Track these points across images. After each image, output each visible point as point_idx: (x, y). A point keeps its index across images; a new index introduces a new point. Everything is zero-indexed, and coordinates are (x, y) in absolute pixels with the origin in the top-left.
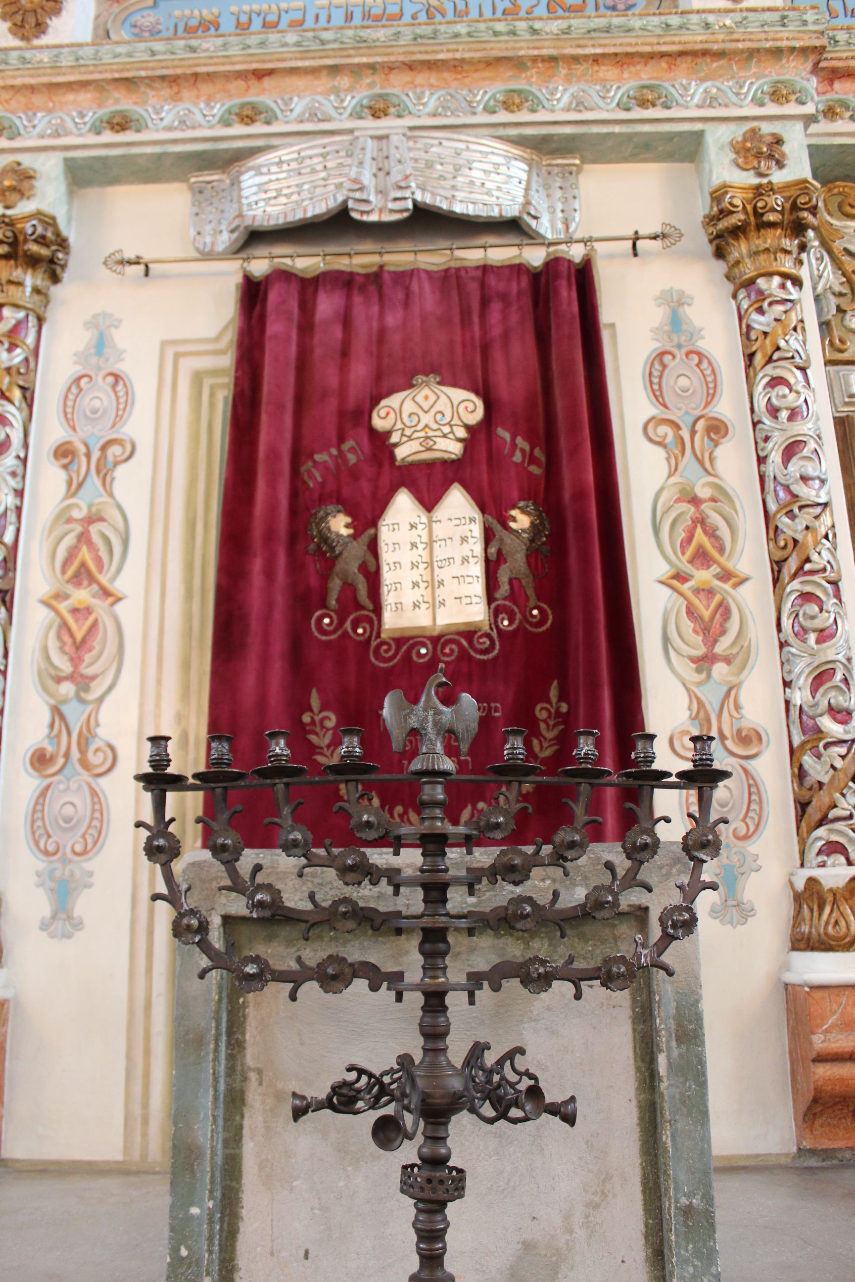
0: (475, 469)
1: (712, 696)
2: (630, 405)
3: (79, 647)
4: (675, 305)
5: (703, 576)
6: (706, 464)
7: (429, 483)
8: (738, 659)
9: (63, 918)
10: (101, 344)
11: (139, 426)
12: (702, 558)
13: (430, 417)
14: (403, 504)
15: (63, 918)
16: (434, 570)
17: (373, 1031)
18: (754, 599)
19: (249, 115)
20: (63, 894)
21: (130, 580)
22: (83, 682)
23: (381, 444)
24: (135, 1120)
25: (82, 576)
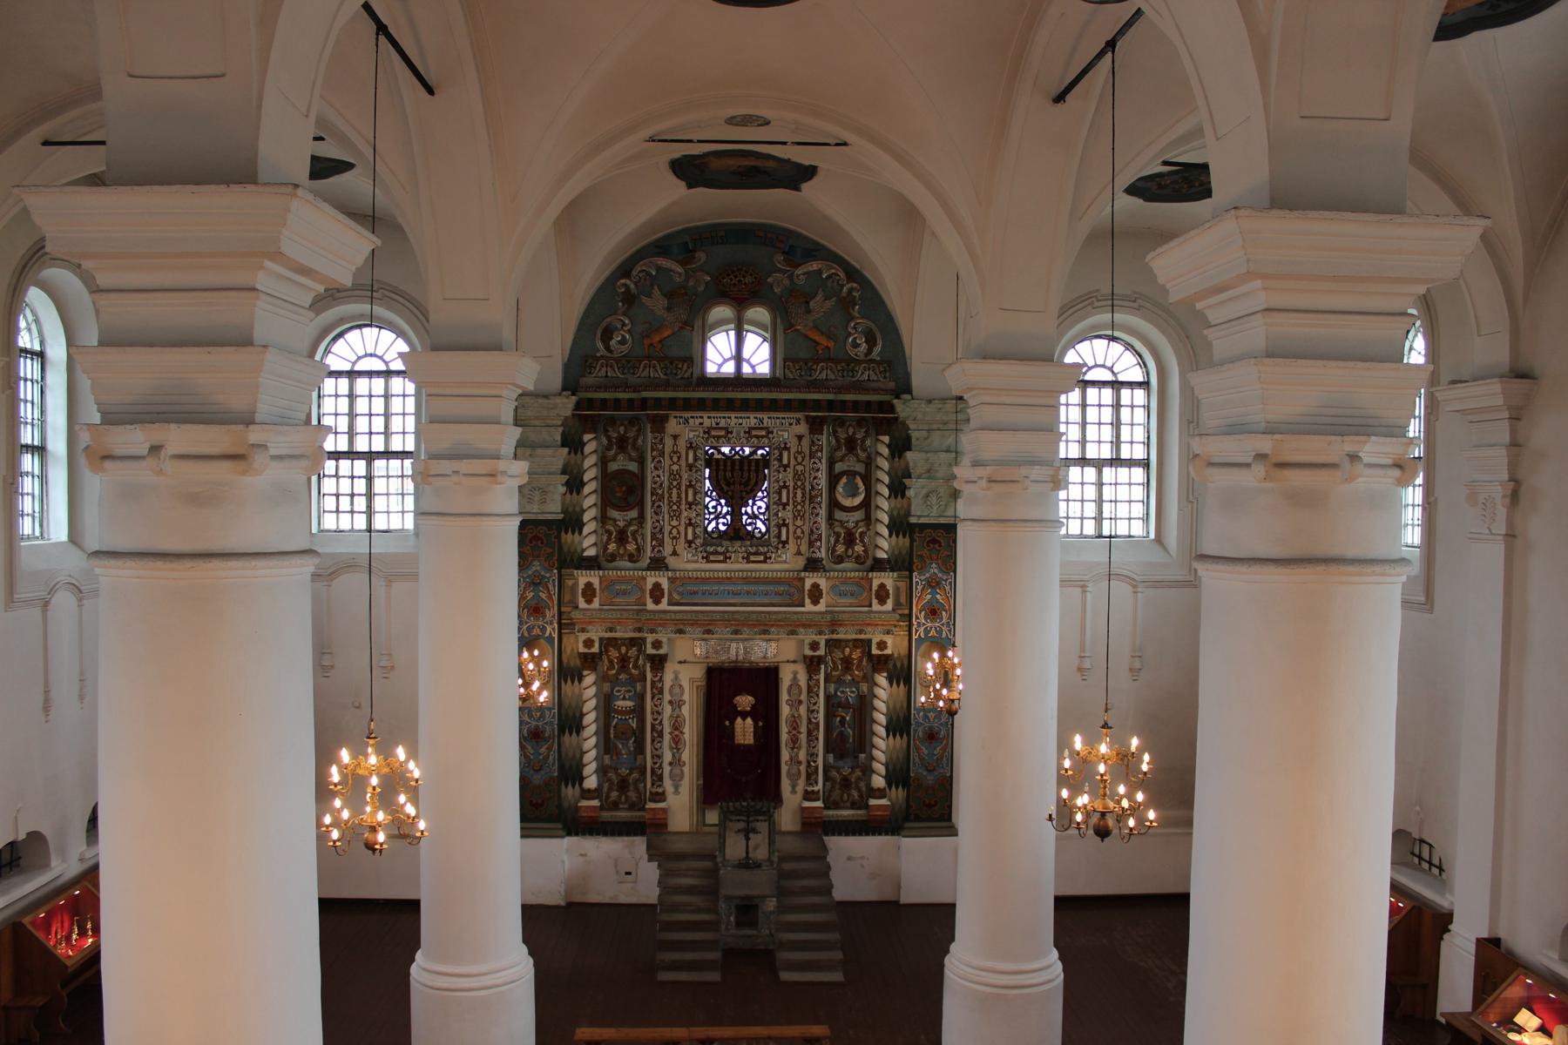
0: (753, 713)
2: (784, 696)
4: (795, 673)
7: (744, 715)
9: (677, 791)
10: (676, 678)
11: (686, 697)
13: (745, 701)
14: (739, 720)
15: (677, 791)
16: (745, 731)
17: (742, 825)
18: (803, 737)
19: (709, 632)
20: (676, 788)
21: (686, 730)
23: (735, 706)
24: (691, 825)
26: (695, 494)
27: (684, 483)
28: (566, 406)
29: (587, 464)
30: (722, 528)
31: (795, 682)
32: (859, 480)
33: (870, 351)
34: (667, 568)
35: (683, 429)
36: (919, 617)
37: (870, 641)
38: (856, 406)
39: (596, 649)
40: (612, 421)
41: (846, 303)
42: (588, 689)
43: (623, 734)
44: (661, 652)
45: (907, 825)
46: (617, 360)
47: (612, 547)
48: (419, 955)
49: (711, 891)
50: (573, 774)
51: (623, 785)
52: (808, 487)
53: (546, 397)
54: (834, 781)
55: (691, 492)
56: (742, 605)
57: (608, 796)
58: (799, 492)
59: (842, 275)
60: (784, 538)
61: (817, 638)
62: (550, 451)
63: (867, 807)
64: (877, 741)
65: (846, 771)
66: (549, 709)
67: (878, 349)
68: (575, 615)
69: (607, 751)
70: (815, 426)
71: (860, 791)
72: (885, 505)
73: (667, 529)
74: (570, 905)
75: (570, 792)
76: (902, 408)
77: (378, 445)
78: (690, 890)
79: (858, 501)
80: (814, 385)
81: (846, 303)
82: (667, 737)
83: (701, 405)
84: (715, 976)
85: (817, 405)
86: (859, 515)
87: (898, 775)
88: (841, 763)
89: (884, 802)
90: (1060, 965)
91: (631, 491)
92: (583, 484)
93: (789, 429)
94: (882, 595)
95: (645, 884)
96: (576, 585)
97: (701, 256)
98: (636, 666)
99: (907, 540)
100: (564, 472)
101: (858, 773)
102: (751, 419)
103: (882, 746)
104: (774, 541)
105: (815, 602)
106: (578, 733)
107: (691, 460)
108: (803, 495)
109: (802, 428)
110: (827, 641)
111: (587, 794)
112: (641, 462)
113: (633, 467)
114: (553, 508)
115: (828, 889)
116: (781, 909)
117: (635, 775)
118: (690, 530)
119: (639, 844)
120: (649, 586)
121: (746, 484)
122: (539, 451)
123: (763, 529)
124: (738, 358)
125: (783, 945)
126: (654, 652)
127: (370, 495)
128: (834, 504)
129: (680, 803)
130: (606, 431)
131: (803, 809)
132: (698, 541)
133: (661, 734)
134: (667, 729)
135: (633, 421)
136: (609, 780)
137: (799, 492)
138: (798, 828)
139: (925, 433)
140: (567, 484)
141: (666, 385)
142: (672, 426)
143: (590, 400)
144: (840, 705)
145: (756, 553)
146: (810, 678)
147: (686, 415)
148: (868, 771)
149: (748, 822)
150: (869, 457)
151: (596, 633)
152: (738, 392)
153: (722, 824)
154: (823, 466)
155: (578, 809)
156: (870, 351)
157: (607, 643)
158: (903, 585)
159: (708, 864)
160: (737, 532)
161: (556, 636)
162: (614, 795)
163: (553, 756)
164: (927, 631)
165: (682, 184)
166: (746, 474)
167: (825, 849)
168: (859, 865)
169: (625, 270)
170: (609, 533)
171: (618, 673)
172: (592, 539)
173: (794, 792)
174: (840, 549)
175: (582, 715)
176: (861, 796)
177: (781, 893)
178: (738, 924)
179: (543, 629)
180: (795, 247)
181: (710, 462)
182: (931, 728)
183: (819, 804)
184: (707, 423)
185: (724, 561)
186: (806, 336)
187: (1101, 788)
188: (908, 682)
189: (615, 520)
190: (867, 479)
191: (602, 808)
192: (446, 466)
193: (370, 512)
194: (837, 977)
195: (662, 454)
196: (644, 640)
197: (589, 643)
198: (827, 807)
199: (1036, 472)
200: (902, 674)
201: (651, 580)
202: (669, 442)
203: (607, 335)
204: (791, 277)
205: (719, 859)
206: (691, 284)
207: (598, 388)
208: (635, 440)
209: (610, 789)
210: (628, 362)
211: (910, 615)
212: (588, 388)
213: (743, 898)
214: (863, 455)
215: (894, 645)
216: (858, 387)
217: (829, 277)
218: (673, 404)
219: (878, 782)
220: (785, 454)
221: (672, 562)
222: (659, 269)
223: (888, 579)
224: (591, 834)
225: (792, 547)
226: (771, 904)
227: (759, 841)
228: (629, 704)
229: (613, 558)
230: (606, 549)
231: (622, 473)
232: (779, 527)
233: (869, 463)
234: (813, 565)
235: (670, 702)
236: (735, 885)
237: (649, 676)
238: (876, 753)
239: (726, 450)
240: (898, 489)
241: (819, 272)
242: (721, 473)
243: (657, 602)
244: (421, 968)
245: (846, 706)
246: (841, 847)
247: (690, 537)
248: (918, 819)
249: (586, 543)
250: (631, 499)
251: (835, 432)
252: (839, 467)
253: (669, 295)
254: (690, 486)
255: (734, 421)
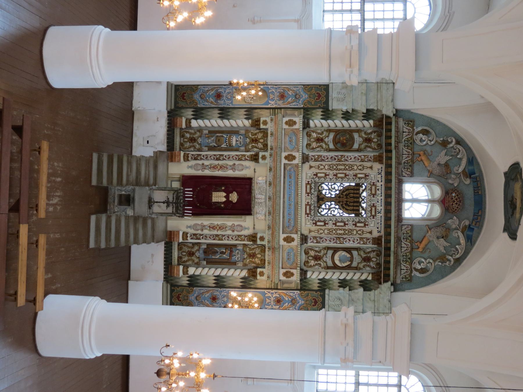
1: (206, 227)
3: (213, 167)
4: (248, 229)
5: (218, 228)
6: (229, 229)
8: (210, 230)
9: (189, 167)
10: (247, 168)
12: (220, 228)
17: (171, 199)
18: (215, 232)
20: (191, 167)
22: (210, 168)
25: (221, 167)
26: (342, 178)
27: (348, 172)
28: (388, 111)
29: (358, 122)
30: (324, 192)
31: (242, 228)
32: (348, 263)
33: (416, 270)
34: (303, 163)
35: (376, 172)
36: (276, 294)
37: (264, 268)
38: (388, 262)
39: (262, 126)
40: (380, 135)
41: (442, 258)
42: (240, 122)
43: (218, 140)
44: (260, 160)
45: (169, 286)
46: (412, 138)
47: (314, 135)
48: (108, 30)
49: (138, 183)
50: (199, 114)
51: (193, 140)
52: (345, 236)
53: (393, 101)
54: (192, 248)
55: (343, 175)
56: (284, 202)
57: (187, 132)
58: (342, 232)
59: (458, 256)
60: (318, 223)
61: (266, 240)
62: (364, 103)
63: (179, 264)
64: (213, 270)
65: (197, 254)
66: (232, 103)
67: (418, 274)
68: (280, 116)
69: (210, 132)
70: (377, 241)
71: (187, 261)
72: (335, 277)
73: (324, 163)
74: (133, 113)
75: (189, 113)
76: (386, 287)
77: (367, 15)
78: (138, 172)
79: (337, 262)
80: (398, 240)
81: (442, 258)
82: (216, 162)
83: (388, 181)
84: (94, 182)
85: (388, 241)
86: (330, 264)
87: (194, 281)
88: (201, 251)
89: (181, 273)
90: (93, 357)
91: (343, 145)
92: (347, 120)
93: (375, 227)
94: (288, 274)
95: (142, 149)
96: (294, 115)
97: (468, 181)
98: (253, 147)
99: (317, 288)
100: (353, 110)
101: (196, 260)
102: (381, 207)
103: (208, 273)
104: (317, 219)
105: (285, 239)
106: (219, 117)
107: (359, 176)
108: (340, 234)
109: (376, 234)
110: (264, 246)
111: (188, 122)
112: (359, 150)
113: (356, 146)
114: (334, 105)
115: (136, 242)
116: (127, 217)
117: (198, 146)
118: (323, 175)
119: (163, 148)
120: (294, 154)
121: (346, 204)
122: (364, 98)
123: (323, 213)
124: (414, 201)
125: (109, 218)
126: (260, 156)
127: (342, 11)
128: (336, 250)
129: (183, 168)
130: (375, 132)
131: (178, 232)
132: (317, 179)
133: (218, 159)
134: (221, 162)
135: (380, 146)
136: (195, 133)
137: (342, 232)
138: (169, 229)
139: (372, 298)
140: (347, 112)
141: (399, 163)
142: (377, 166)
143: (390, 124)
144: (231, 251)
145: (310, 209)
146: (245, 236)
147: (383, 174)
148: (197, 265)
149: (172, 203)
150: (360, 269)
151: (270, 127)
152: (393, 200)
153: (171, 189)
154: (355, 245)
155: (181, 117)
156: (416, 270)
157: (265, 133)
158: (293, 286)
159: (151, 181)
160: (321, 199)
161: (269, 106)
162: (188, 135)
163: (207, 104)
164: (269, 298)
165: (506, 169)
166: (351, 204)
167: (158, 242)
168: (148, 260)
169: (460, 142)
170: (322, 133)
171: (249, 138)
172: (319, 125)
173: (188, 227)
174: (312, 253)
175: (228, 119)
176: (184, 262)
177: (136, 219)
178: (120, 196)
179: (272, 100)
180: (472, 232)
181: (358, 185)
182: (218, 299)
183: (181, 240)
184: (379, 184)
185: (306, 193)
186: (425, 237)
187: (182, 373)
188: (243, 287)
189: (328, 137)
190: (349, 267)
191: (181, 129)
192: (355, 42)
193: (334, 11)
194: (92, 245)
195: (362, 161)
196: (266, 151)
197: (265, 123)
198: (179, 244)
199: (350, 349)
200: (246, 285)
201: (298, 155)
202: (369, 164)
203: (425, 132)
204: (456, 229)
205: (154, 187)
206: (453, 176)
207: (397, 127)
208: (370, 147)
209: (191, 134)
210: (410, 143)
211: (277, 289)
212: (397, 122)
213: (133, 198)
214: (361, 266)
215: (262, 281)
216: (397, 263)
217: (457, 250)
218: (389, 166)
219: (191, 271)
220: (362, 225)
221: (307, 165)
222: (461, 159)
223: (296, 277)
224: (168, 123)
225: (314, 228)
226: (130, 212)
227: (163, 208)
228: (234, 143)
229: (309, 135)
230: (313, 132)
231: (352, 139)
232: (324, 221)
233: (356, 268)
234: (304, 239)
235: (234, 164)
236: (141, 196)
237: (248, 154)
238: (206, 270)
239: (364, 194)
240: (343, 284)
241: (459, 244)
242: (352, 191)
243: (286, 158)
244: (101, 31)
245: (231, 255)
246: (158, 250)
247: (319, 175)
248: (172, 291)
249: (317, 122)
250: (339, 145)
251: (374, 251)
252: (355, 253)
253: (447, 165)
254: (346, 175)
255: (380, 198)
